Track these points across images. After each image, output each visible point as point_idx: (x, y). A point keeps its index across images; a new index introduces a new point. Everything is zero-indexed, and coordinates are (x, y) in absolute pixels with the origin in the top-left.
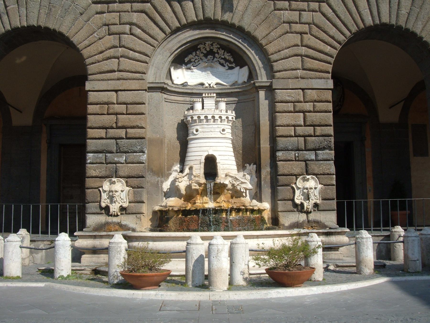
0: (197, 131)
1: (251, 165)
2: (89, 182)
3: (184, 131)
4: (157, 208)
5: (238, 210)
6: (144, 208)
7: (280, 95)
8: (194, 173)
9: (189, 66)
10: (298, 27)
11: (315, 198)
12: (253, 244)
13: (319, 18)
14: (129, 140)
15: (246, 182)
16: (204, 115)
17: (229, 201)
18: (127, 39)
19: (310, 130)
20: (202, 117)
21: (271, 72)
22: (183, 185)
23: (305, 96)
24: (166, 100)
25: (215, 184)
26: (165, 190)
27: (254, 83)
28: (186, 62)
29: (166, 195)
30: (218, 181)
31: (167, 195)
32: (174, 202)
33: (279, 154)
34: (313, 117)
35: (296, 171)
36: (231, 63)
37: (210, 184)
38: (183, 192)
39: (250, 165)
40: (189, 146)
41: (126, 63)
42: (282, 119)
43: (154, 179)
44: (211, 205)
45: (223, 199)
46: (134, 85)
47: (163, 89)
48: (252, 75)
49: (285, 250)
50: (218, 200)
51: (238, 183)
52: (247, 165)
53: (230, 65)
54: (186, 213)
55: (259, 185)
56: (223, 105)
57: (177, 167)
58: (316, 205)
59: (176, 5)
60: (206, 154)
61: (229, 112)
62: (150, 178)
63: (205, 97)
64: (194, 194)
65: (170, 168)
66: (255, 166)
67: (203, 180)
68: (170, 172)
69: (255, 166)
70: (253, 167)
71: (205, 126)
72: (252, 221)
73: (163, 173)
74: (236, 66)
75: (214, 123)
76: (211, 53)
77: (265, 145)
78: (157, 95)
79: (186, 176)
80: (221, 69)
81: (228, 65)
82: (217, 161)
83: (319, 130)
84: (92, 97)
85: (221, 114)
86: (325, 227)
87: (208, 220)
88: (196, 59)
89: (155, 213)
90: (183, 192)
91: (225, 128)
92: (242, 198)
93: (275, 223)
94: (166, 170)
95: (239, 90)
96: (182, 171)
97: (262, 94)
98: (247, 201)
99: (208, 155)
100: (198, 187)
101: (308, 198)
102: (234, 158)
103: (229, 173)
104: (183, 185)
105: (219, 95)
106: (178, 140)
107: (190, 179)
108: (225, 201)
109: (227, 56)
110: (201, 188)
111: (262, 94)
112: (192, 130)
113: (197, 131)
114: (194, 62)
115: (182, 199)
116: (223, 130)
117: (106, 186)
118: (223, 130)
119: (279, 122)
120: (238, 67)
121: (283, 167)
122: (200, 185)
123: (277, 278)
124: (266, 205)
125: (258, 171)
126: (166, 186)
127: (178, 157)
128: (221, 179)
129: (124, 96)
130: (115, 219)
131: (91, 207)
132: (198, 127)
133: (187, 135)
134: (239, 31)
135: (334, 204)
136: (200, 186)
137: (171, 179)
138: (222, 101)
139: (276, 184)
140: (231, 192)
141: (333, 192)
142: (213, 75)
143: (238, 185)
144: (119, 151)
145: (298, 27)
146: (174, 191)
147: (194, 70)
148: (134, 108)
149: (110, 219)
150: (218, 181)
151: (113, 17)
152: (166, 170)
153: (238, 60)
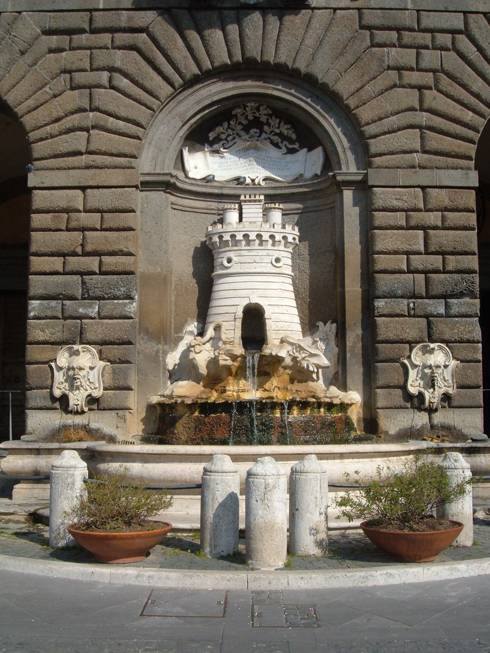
0: (229, 261)
1: (328, 324)
2: (33, 352)
3: (206, 263)
4: (155, 399)
5: (304, 405)
7: (382, 196)
8: (223, 337)
9: (216, 147)
10: (414, 77)
11: (445, 384)
12: (336, 469)
13: (452, 61)
14: (105, 276)
15: (318, 355)
16: (243, 233)
17: (287, 389)
18: (105, 97)
19: (437, 261)
20: (239, 237)
22: (202, 358)
24: (174, 207)
25: (262, 357)
26: (170, 367)
27: (334, 176)
28: (211, 139)
29: (174, 377)
30: (267, 351)
31: (174, 376)
32: (186, 389)
33: (380, 304)
35: (411, 334)
36: (291, 142)
37: (253, 357)
38: (203, 371)
39: (325, 324)
40: (216, 288)
41: (101, 140)
42: (384, 240)
43: (151, 347)
45: (275, 384)
46: (115, 177)
47: (168, 186)
48: (330, 162)
50: (267, 386)
51: (304, 355)
52: (321, 324)
53: (290, 146)
54: (207, 408)
55: (341, 360)
56: (277, 216)
57: (193, 327)
58: (446, 397)
59: (193, 36)
60: (245, 302)
61: (289, 228)
62: (143, 345)
63: (245, 201)
64: (224, 374)
65: (180, 328)
66: (334, 325)
67: (239, 350)
68: (180, 335)
69: (334, 325)
70: (331, 328)
71: (245, 253)
73: (168, 337)
74: (301, 147)
75: (260, 248)
76: (255, 125)
77: (353, 287)
78: (157, 197)
79: (208, 341)
80: (274, 153)
81: (286, 146)
82: (266, 316)
83: (452, 262)
84: (40, 199)
85: (273, 230)
86: (463, 437)
88: (229, 135)
89: (151, 408)
90: (203, 371)
91: (280, 257)
92: (311, 383)
93: (371, 429)
94: (173, 332)
95: (306, 190)
96: (201, 333)
97: (348, 195)
99: (250, 303)
100: (229, 362)
101: (431, 383)
102: (295, 311)
103: (286, 336)
105: (270, 198)
106: (194, 277)
107: (216, 347)
108: (279, 388)
109: (285, 129)
110: (236, 364)
111: (348, 195)
112: (219, 260)
113: (229, 261)
114: (226, 139)
115: (201, 383)
116: (278, 260)
117: (63, 359)
118: (278, 260)
119: (379, 246)
120: (305, 150)
121: (386, 328)
122: (234, 358)
124: (355, 397)
125: (341, 335)
126: (173, 359)
127: (194, 308)
128: (273, 347)
129: (98, 198)
130: (78, 420)
131: (36, 397)
132: (231, 255)
133: (212, 269)
134: (308, 82)
135: (478, 395)
136: (233, 361)
137: (182, 347)
138: (275, 208)
140: (290, 372)
141: (476, 373)
142: (259, 164)
143: (303, 359)
144: (88, 296)
145: (414, 77)
146: (186, 369)
147: (225, 154)
148: (116, 218)
149: (70, 420)
150: (267, 351)
151: (81, 58)
152: (173, 332)
153: (304, 135)
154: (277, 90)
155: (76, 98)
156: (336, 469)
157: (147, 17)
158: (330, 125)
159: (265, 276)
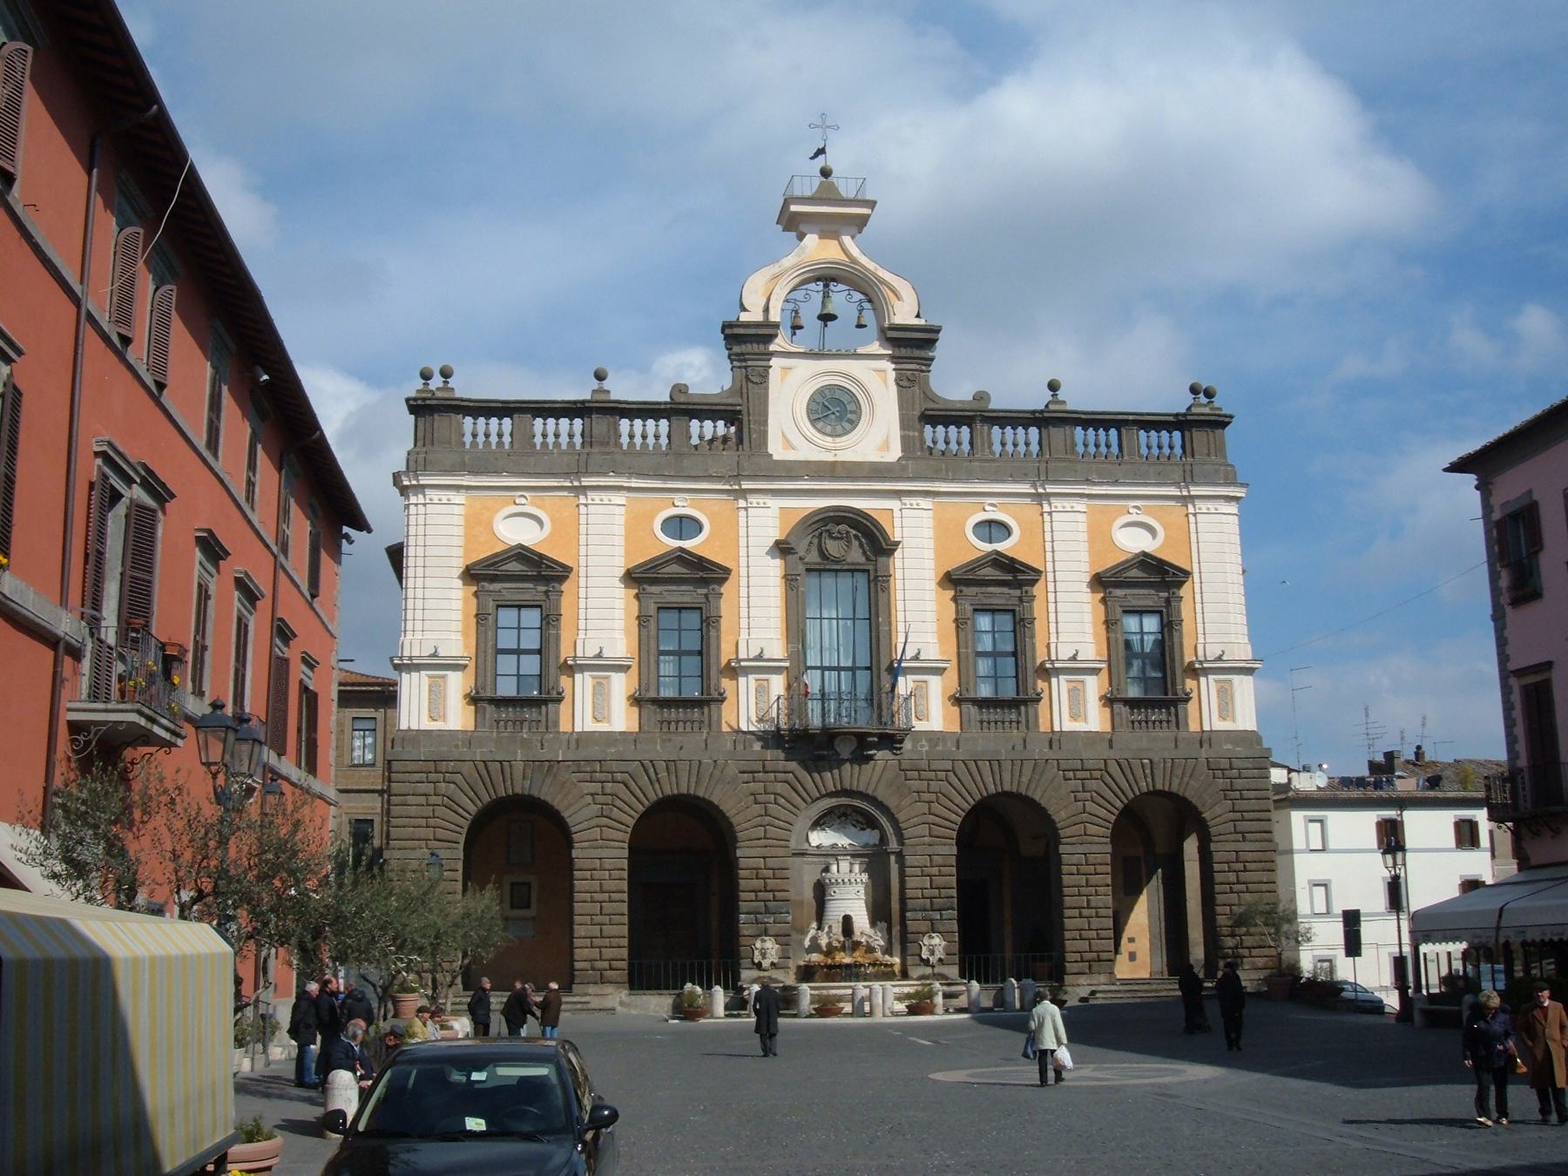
2: (743, 941)
3: (821, 892)
6: (792, 964)
7: (909, 860)
10: (926, 796)
11: (939, 954)
12: (897, 990)
14: (775, 903)
15: (879, 941)
21: (901, 839)
22: (824, 941)
23: (932, 861)
31: (809, 951)
32: (816, 957)
33: (908, 914)
34: (939, 881)
35: (924, 929)
42: (911, 882)
43: (795, 936)
44: (848, 960)
46: (780, 852)
48: (883, 839)
49: (917, 993)
54: (830, 967)
55: (890, 942)
56: (856, 868)
57: (814, 925)
59: (816, 775)
62: (795, 936)
70: (884, 925)
72: (886, 974)
73: (804, 932)
76: (844, 815)
78: (797, 859)
84: (743, 863)
86: (946, 978)
87: (851, 973)
89: (799, 967)
93: (905, 975)
97: (893, 858)
98: (879, 954)
101: (932, 953)
104: (824, 941)
105: (853, 856)
111: (893, 858)
117: (758, 944)
119: (908, 885)
121: (912, 926)
123: (912, 1010)
124: (897, 960)
126: (807, 943)
128: (857, 937)
129: (771, 862)
131: (745, 962)
134: (873, 800)
135: (956, 959)
139: (905, 941)
141: (956, 948)
144: (767, 911)
145: (926, 796)
146: (815, 947)
148: (780, 872)
149: (762, 974)
151: (759, 787)
153: (870, 823)
154: (857, 803)
155: (758, 809)
156: (897, 990)
157: (793, 765)
158: (883, 821)
159: (851, 900)
